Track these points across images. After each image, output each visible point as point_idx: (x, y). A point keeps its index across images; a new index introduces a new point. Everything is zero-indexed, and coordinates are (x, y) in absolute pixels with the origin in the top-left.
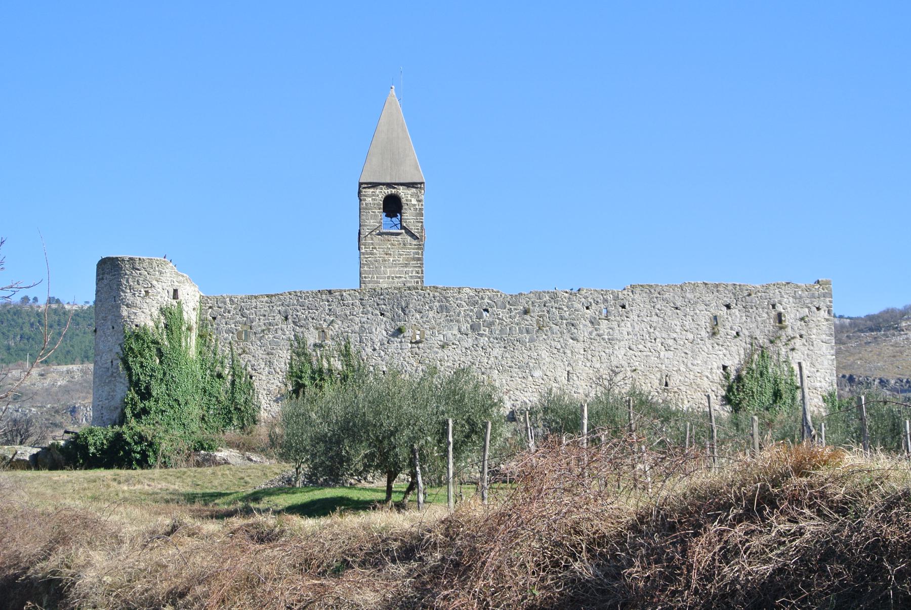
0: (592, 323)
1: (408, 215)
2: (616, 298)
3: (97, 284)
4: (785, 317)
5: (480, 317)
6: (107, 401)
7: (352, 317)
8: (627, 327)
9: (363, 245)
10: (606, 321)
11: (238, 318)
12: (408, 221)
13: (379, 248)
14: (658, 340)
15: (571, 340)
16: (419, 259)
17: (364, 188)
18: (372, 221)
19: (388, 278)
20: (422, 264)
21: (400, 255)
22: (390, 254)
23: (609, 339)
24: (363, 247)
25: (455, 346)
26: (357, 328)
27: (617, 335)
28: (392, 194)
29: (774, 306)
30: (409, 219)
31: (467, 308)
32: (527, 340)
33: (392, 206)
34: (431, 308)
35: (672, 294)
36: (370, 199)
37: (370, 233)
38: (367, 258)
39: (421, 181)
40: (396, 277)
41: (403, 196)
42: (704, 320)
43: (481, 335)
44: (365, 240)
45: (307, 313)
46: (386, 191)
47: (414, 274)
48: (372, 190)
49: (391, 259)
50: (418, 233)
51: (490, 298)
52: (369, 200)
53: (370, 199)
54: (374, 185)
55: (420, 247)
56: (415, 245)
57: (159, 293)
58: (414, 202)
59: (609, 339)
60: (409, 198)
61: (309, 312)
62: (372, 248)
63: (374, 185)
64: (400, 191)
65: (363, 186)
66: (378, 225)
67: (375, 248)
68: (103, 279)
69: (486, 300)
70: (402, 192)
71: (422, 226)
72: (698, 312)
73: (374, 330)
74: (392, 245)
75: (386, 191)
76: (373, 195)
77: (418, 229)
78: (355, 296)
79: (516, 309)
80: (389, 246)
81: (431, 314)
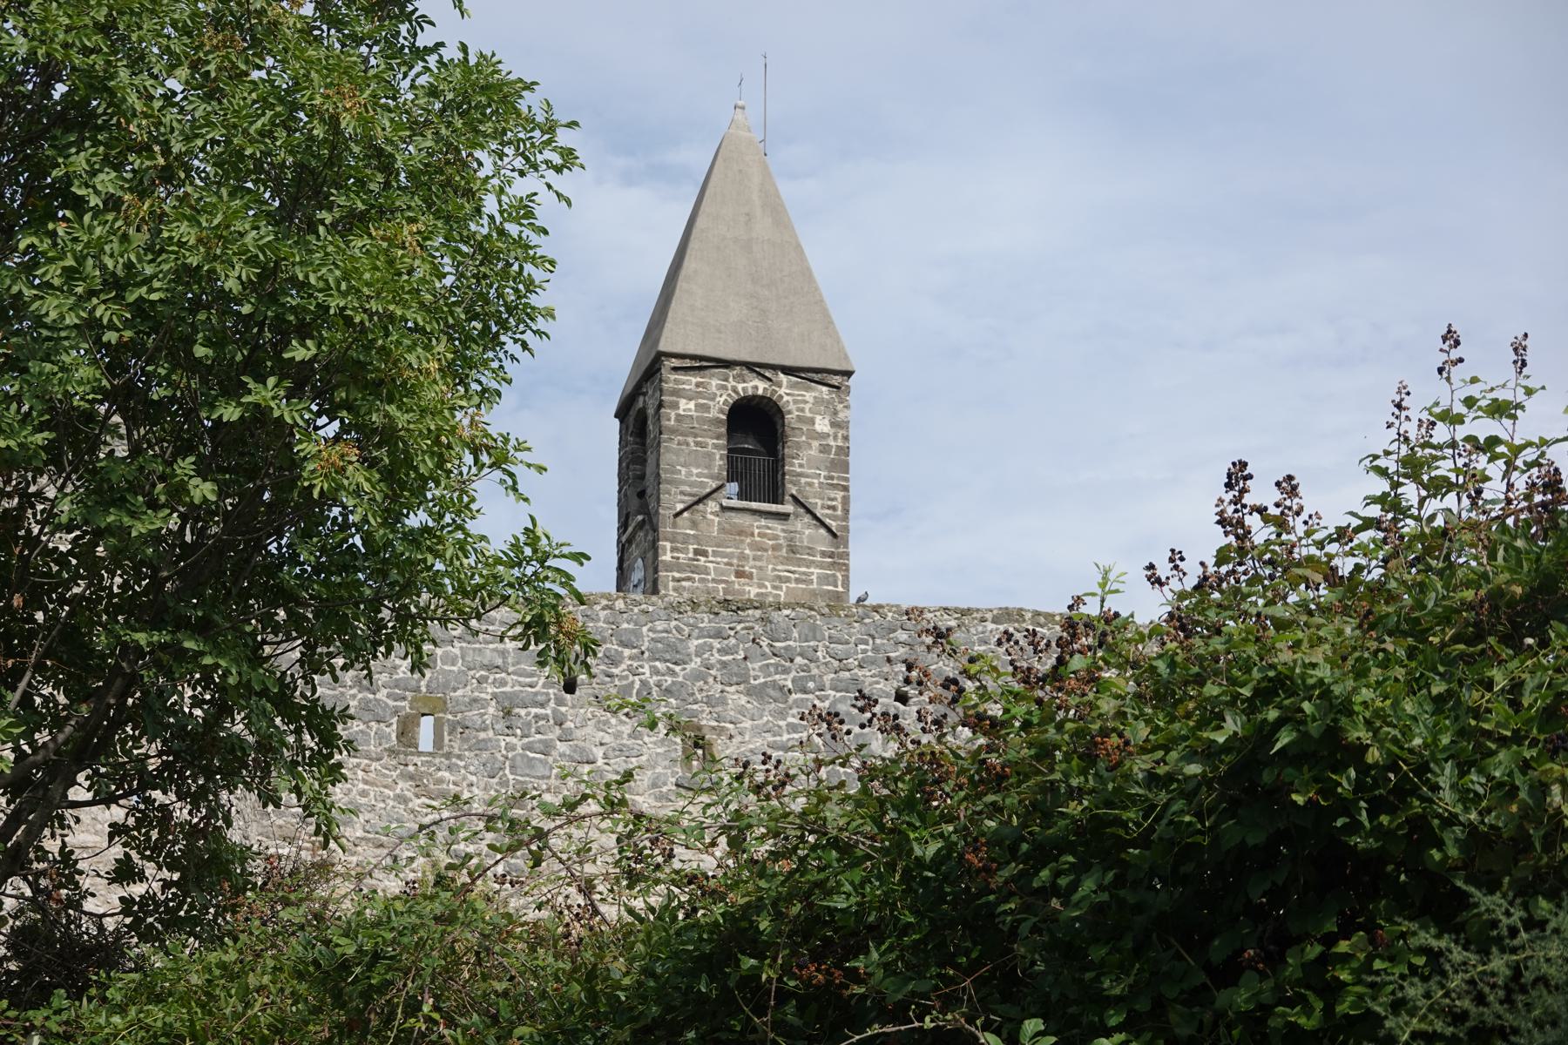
7: (799, 696)
9: (666, 540)
12: (803, 480)
13: (715, 554)
17: (675, 369)
18: (695, 471)
21: (780, 578)
22: (750, 576)
24: (668, 545)
28: (754, 397)
30: (807, 476)
36: (692, 405)
38: (679, 580)
39: (844, 367)
41: (792, 407)
44: (674, 525)
45: (646, 670)
46: (740, 387)
48: (694, 380)
50: (835, 518)
52: (686, 406)
53: (692, 405)
56: (824, 554)
58: (822, 425)
60: (808, 414)
61: (655, 671)
62: (697, 552)
64: (782, 391)
65: (675, 363)
67: (704, 554)
70: (786, 391)
71: (846, 501)
75: (740, 387)
76: (699, 395)
77: (834, 508)
78: (814, 628)
80: (747, 552)
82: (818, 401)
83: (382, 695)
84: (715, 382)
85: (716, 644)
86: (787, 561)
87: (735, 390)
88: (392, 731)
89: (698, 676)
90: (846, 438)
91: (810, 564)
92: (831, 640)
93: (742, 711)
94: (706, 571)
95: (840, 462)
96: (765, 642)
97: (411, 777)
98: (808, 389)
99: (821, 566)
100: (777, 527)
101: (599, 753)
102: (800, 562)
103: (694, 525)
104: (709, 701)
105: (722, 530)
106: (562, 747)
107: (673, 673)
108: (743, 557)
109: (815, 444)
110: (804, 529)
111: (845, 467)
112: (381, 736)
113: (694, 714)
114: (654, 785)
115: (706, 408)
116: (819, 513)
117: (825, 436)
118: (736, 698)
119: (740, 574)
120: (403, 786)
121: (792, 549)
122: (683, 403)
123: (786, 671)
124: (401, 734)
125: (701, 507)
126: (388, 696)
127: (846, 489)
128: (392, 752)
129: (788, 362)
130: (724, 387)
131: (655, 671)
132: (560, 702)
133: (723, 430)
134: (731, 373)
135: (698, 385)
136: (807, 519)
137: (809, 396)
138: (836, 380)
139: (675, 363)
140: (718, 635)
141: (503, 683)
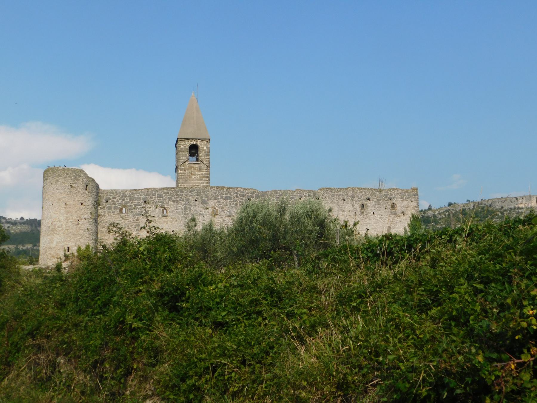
1: (202, 155)
2: (314, 194)
4: (396, 205)
6: (49, 244)
16: (208, 177)
20: (209, 179)
26: (183, 207)
31: (240, 198)
33: (194, 150)
34: (222, 198)
42: (358, 207)
51: (251, 193)
52: (182, 147)
54: (185, 139)
55: (208, 171)
57: (78, 187)
58: (205, 148)
61: (158, 199)
63: (185, 139)
64: (198, 143)
65: (180, 139)
68: (47, 179)
69: (250, 194)
70: (199, 143)
71: (209, 161)
74: (194, 169)
81: (222, 201)
82: (204, 144)
83: (117, 205)
84: (187, 142)
85: (167, 194)
86: (199, 171)
88: (119, 211)
89: (164, 199)
90: (209, 150)
91: (203, 172)
93: (171, 204)
94: (186, 174)
95: (208, 154)
96: (175, 194)
97: (122, 217)
99: (205, 172)
100: (197, 166)
102: (201, 171)
103: (184, 166)
104: (167, 203)
105: (188, 167)
107: (160, 199)
108: (192, 171)
109: (204, 151)
110: (202, 166)
111: (209, 155)
112: (117, 211)
115: (185, 147)
117: (205, 150)
118: (171, 202)
119: (191, 174)
120: (121, 219)
121: (200, 169)
123: (178, 198)
128: (119, 214)
129: (199, 138)
131: (158, 199)
132: (144, 205)
134: (189, 141)
137: (203, 143)
138: (207, 140)
139: (180, 139)
140: (168, 193)
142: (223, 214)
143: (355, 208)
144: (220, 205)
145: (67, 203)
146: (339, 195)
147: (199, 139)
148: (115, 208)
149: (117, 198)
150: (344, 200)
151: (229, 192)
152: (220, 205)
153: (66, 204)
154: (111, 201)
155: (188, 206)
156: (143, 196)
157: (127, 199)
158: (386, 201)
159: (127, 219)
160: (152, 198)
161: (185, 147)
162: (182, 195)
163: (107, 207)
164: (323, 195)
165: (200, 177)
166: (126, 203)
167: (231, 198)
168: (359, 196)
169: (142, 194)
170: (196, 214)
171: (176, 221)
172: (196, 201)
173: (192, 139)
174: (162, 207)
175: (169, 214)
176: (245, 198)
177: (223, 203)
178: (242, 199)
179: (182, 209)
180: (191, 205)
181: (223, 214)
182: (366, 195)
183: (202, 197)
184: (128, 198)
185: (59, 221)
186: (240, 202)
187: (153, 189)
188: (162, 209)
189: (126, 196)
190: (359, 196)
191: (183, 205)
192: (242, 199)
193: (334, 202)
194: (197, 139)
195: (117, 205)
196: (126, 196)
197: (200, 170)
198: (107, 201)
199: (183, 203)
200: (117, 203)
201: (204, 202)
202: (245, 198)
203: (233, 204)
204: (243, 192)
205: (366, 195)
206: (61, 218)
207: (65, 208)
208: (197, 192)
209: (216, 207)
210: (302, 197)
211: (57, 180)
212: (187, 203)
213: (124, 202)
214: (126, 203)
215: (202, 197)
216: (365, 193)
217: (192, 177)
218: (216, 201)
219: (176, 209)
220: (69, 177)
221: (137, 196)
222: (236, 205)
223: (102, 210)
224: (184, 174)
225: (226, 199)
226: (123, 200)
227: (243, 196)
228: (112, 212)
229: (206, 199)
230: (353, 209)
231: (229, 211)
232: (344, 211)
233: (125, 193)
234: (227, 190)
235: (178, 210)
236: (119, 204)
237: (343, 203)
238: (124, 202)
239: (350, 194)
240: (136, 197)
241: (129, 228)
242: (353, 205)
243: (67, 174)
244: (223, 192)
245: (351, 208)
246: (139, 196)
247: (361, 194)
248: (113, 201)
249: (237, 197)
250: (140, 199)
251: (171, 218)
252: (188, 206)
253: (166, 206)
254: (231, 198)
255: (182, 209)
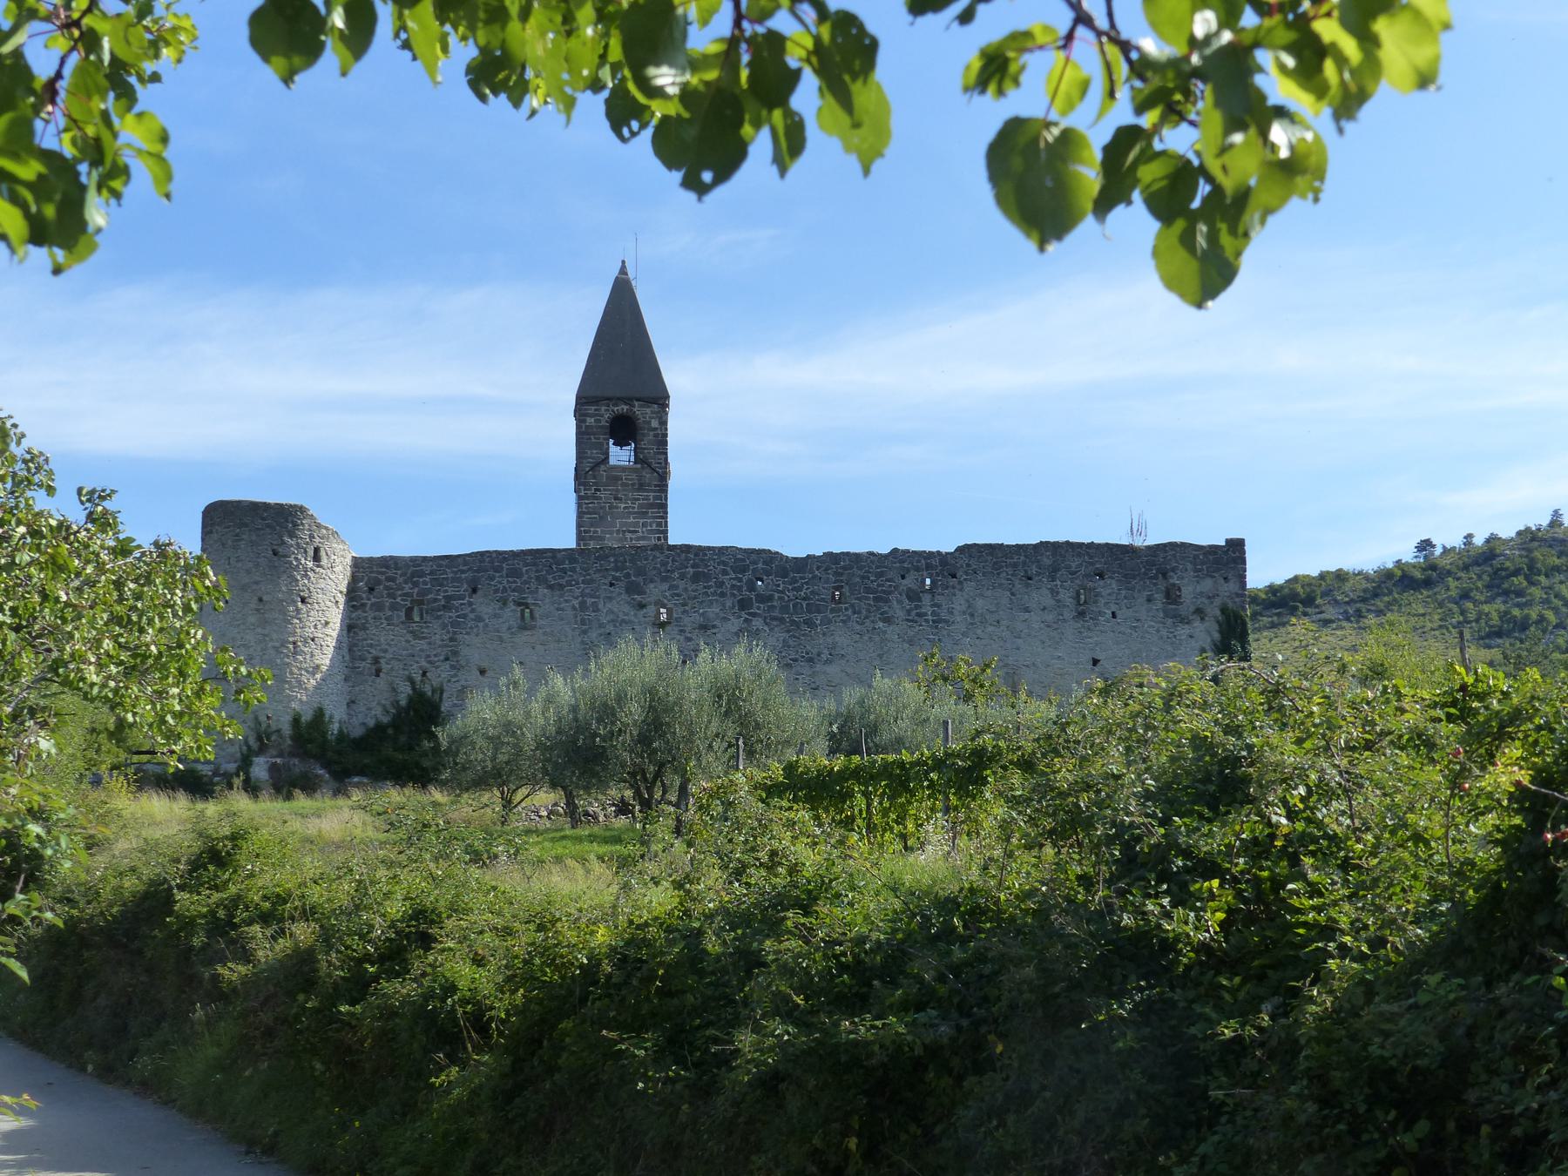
0: (909, 598)
1: (647, 440)
3: (203, 540)
5: (752, 587)
8: (959, 603)
10: (930, 596)
11: (407, 588)
13: (605, 490)
14: (1002, 622)
15: (881, 624)
19: (618, 532)
23: (934, 621)
24: (582, 488)
25: (714, 631)
26: (576, 603)
27: (944, 615)
29: (1165, 575)
32: (819, 622)
34: (682, 577)
35: (1022, 558)
36: (593, 420)
37: (592, 469)
40: (630, 532)
41: (640, 416)
42: (1066, 596)
43: (754, 615)
45: (505, 582)
47: (654, 527)
49: (623, 506)
51: (764, 563)
52: (590, 421)
53: (593, 420)
56: (656, 486)
58: (655, 424)
59: (934, 621)
63: (596, 401)
66: (603, 457)
67: (599, 490)
68: (211, 532)
72: (1059, 583)
73: (601, 606)
76: (597, 415)
79: (801, 578)
81: (682, 584)
82: (652, 412)
83: (399, 600)
84: (603, 408)
85: (534, 569)
87: (613, 411)
88: (403, 614)
89: (526, 582)
91: (648, 491)
92: (583, 563)
93: (545, 595)
94: (601, 498)
96: (554, 567)
97: (411, 632)
98: (649, 407)
101: (486, 617)
103: (594, 477)
105: (607, 478)
106: (472, 616)
107: (515, 582)
108: (617, 491)
109: (652, 433)
112: (398, 616)
113: (524, 598)
114: (509, 629)
115: (600, 421)
116: (654, 465)
117: (656, 429)
118: (543, 591)
121: (641, 485)
122: (588, 419)
123: (563, 578)
124: (406, 615)
125: (597, 468)
126: (402, 600)
127: (666, 453)
128: (402, 623)
130: (608, 410)
132: (470, 597)
133: (608, 431)
135: (596, 410)
136: (648, 470)
137: (648, 410)
140: (535, 564)
141: (446, 591)
142: (686, 620)
143: (1059, 601)
144: (678, 595)
145: (265, 598)
146: (1015, 565)
147: (638, 400)
148: (394, 607)
149: (400, 580)
150: (1030, 579)
151: (702, 560)
152: (678, 595)
153: (261, 600)
154: (381, 587)
155: (589, 601)
156: (469, 575)
157: (425, 583)
158: (1151, 578)
159: (424, 638)
160: (492, 579)
161: (600, 421)
162: (573, 570)
163: (372, 605)
164: (968, 565)
165: (641, 506)
166: (423, 593)
167: (707, 577)
168: (1073, 565)
169: (465, 568)
170: (613, 621)
171: (559, 641)
172: (612, 585)
173: (618, 399)
174: (519, 604)
175: (540, 622)
176: (748, 575)
177: (686, 589)
178: (740, 580)
179: (574, 608)
180: (598, 597)
181: (686, 620)
182: (1092, 564)
183: (628, 575)
184: (427, 579)
185: (244, 645)
186: (733, 586)
187: (494, 555)
188: (519, 609)
189: (422, 574)
190: (1073, 565)
191: (577, 598)
192: (740, 580)
193: (1001, 585)
194: (631, 399)
195: (399, 600)
196: (422, 574)
197: (641, 487)
198: (371, 590)
199: (577, 592)
200: (400, 592)
201: (632, 589)
202: (748, 575)
203: (714, 594)
204: (744, 560)
205: (1092, 564)
206: (248, 637)
207: (257, 610)
208: (616, 561)
209: (665, 601)
210: (908, 570)
211: (237, 535)
212: (587, 591)
213: (416, 590)
214: (423, 593)
215: (628, 575)
216: (1091, 557)
217: (617, 508)
218: (665, 586)
219: (558, 609)
220: (268, 526)
221: (453, 572)
222: (723, 595)
223: (359, 612)
224: (597, 498)
225: (696, 578)
226: (415, 584)
227: (744, 570)
228: (386, 619)
229: (640, 579)
230: (1053, 602)
231: (703, 614)
232: (1027, 610)
233: (420, 565)
234: (696, 555)
235: (562, 610)
236: (405, 595)
237: (1027, 586)
238: (416, 590)
239: (1047, 561)
240: (450, 575)
241: (430, 662)
242: (1055, 593)
243: (264, 519)
244: (688, 559)
245: (1049, 601)
246: (456, 573)
247: (1077, 561)
248: (387, 588)
249: (725, 573)
250: (459, 580)
251: (545, 634)
252: (589, 601)
253: (530, 601)
254: (707, 577)
255: (574, 608)
